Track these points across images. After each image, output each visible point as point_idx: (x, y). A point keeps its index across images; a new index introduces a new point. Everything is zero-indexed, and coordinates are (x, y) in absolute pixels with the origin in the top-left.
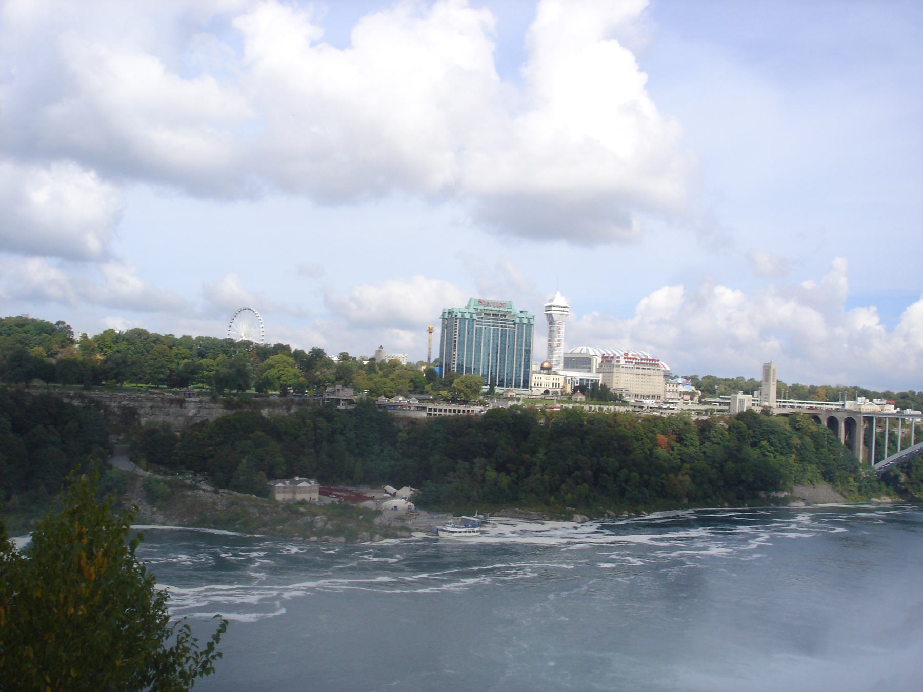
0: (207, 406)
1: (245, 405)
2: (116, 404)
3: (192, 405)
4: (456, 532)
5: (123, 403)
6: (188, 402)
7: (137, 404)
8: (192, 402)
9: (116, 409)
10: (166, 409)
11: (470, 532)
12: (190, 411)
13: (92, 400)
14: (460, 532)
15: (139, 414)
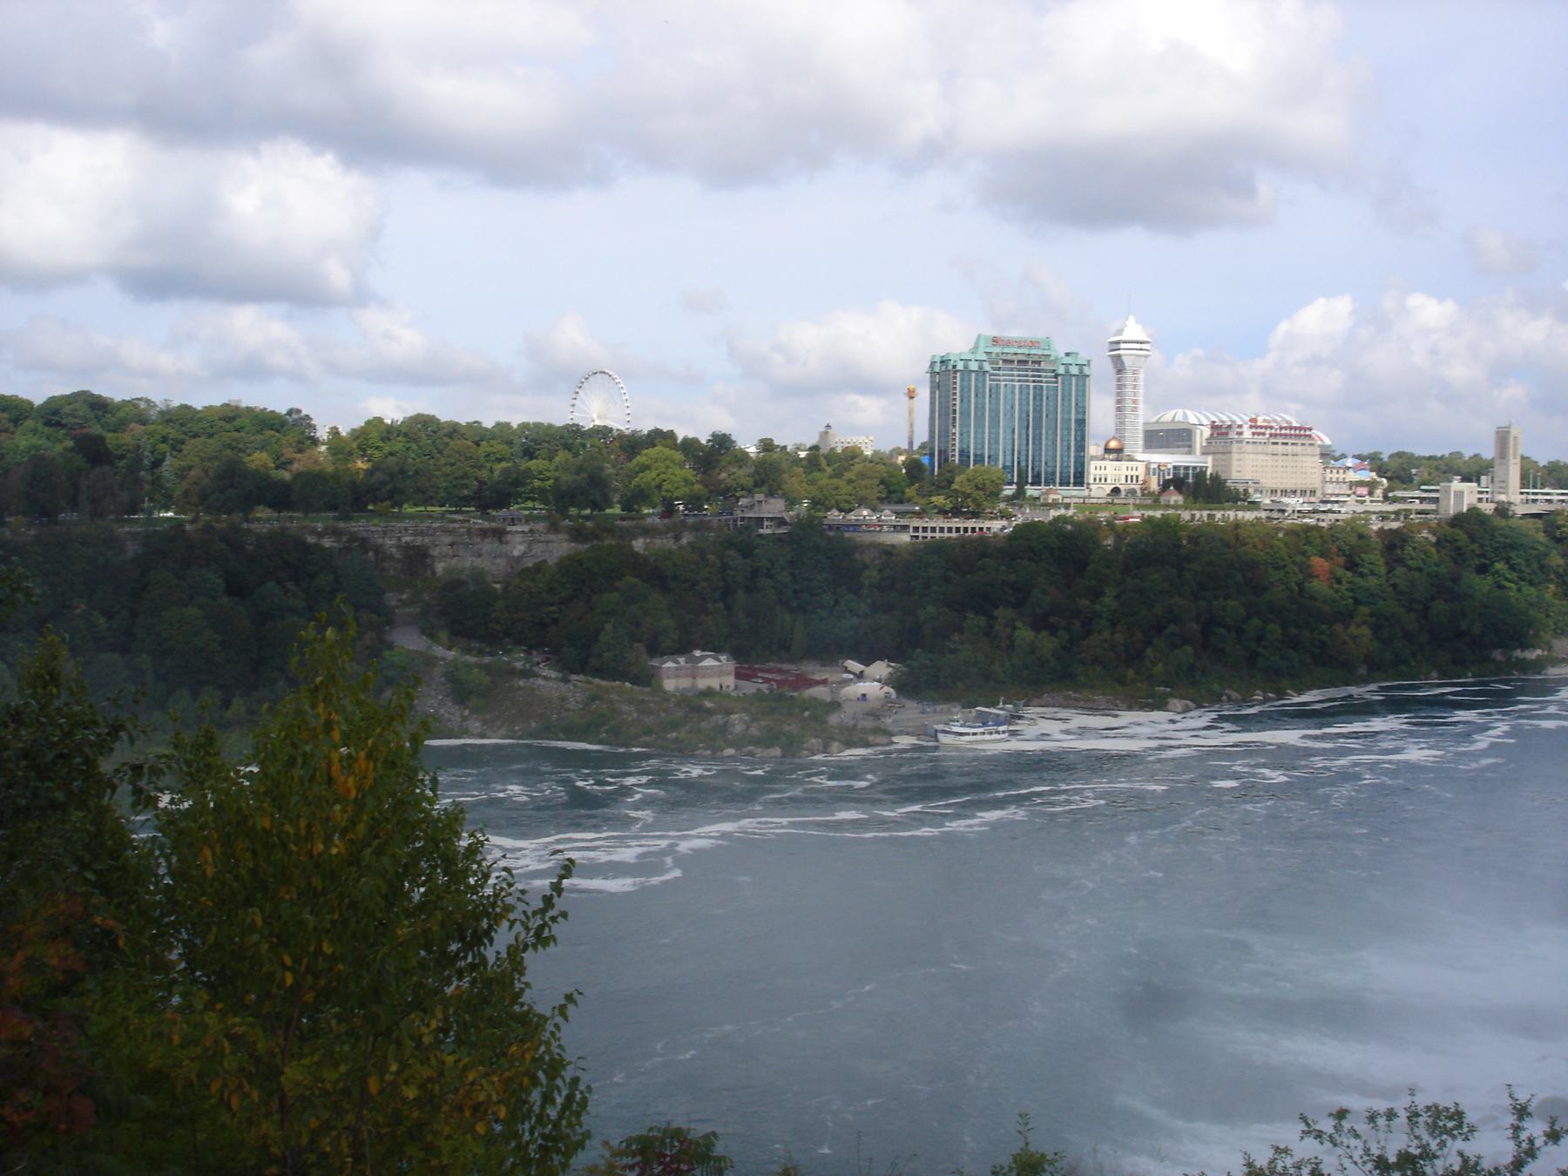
0: (542, 539)
1: (605, 534)
2: (392, 542)
3: (518, 538)
4: (968, 734)
5: (404, 539)
6: (510, 532)
7: (427, 540)
8: (516, 532)
9: (394, 550)
10: (476, 547)
11: (991, 733)
12: (514, 548)
13: (353, 537)
14: (974, 734)
15: (432, 556)
